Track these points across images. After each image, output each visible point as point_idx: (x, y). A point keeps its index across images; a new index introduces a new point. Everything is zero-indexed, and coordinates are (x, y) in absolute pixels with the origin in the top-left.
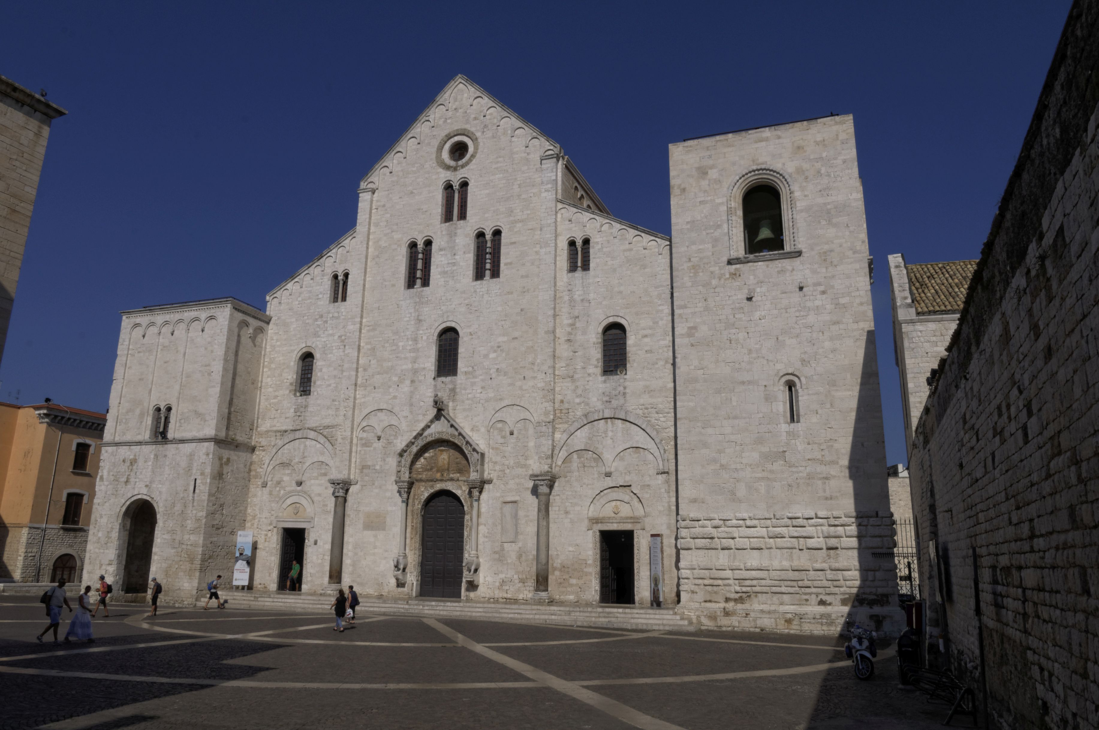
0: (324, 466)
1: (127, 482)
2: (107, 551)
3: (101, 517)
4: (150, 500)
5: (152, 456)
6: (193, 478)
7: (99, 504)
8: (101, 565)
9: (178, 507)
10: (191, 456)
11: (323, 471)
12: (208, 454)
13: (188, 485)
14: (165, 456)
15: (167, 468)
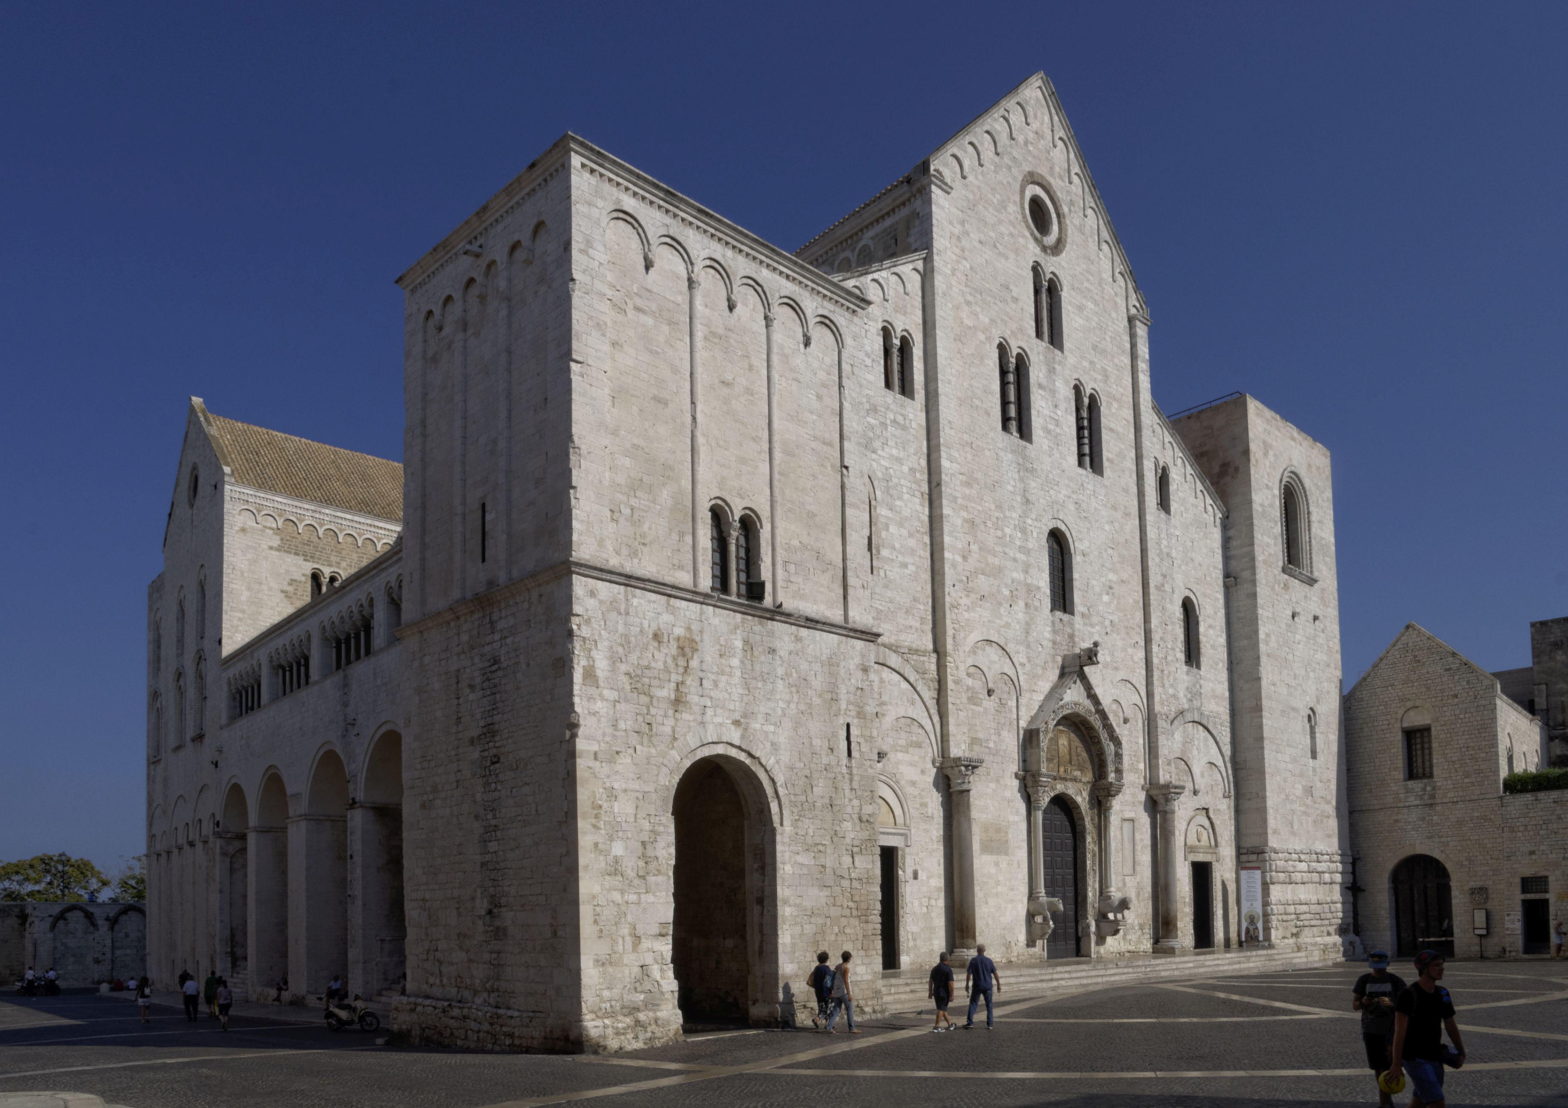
0: (915, 729)
1: (678, 702)
2: (650, 898)
3: (612, 795)
4: (748, 761)
5: (739, 644)
6: (842, 721)
7: (596, 756)
8: (637, 939)
9: (821, 789)
10: (831, 664)
11: (914, 739)
12: (865, 670)
13: (834, 735)
14: (772, 651)
15: (780, 685)
